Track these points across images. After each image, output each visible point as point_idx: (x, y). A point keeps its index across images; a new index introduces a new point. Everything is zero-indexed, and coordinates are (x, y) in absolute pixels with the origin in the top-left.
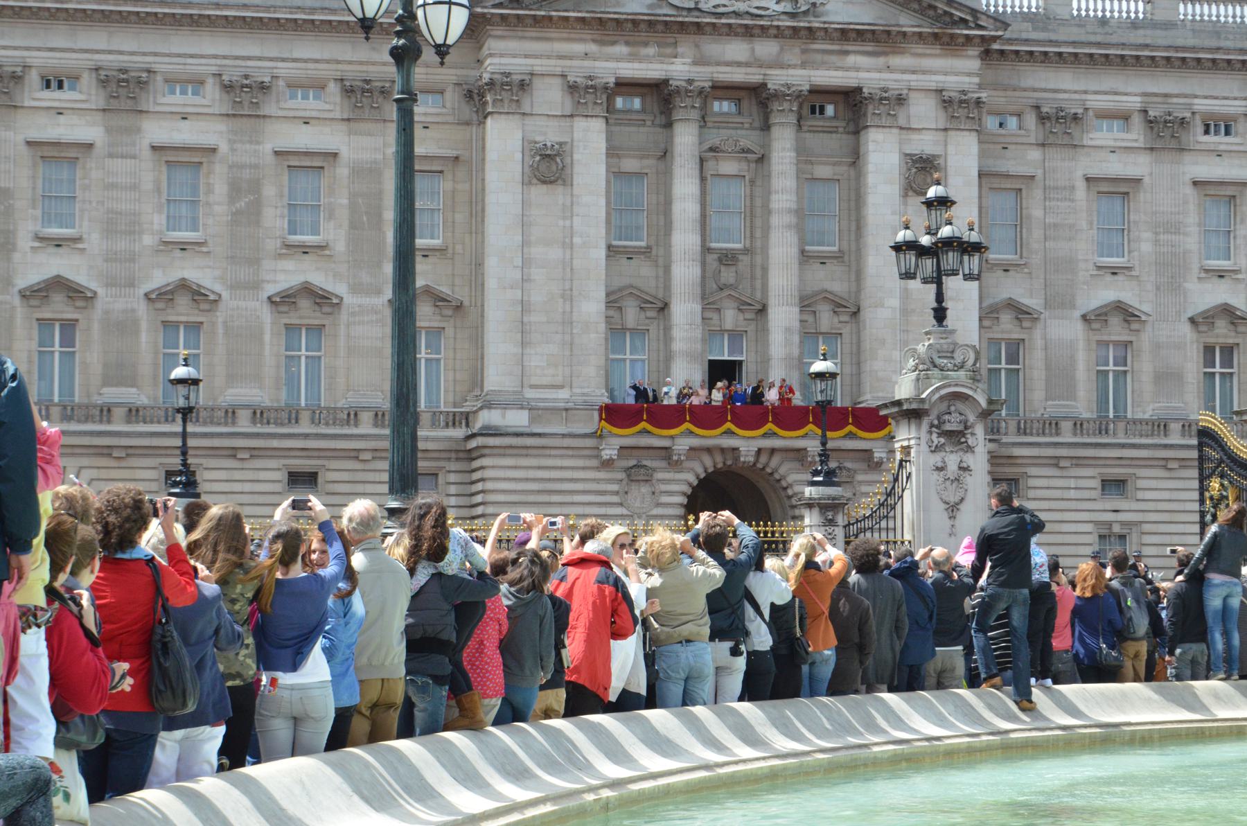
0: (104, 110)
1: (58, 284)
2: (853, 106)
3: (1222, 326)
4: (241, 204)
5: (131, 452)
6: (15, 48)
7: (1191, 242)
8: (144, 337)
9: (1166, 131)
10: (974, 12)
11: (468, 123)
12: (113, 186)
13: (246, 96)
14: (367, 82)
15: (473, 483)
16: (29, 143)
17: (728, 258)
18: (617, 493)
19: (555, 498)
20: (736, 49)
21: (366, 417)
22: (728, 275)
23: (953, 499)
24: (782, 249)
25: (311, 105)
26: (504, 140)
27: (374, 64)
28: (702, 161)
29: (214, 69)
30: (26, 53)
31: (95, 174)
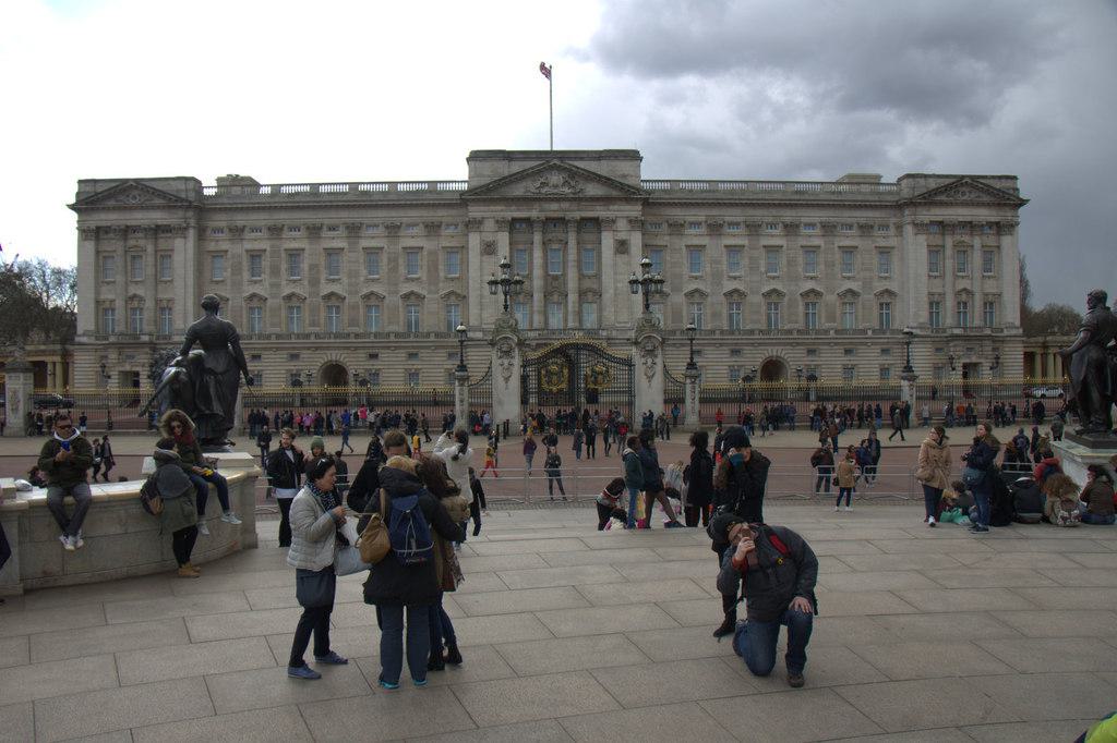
1: (332, 294)
2: (597, 223)
3: (735, 296)
5: (356, 349)
7: (725, 267)
8: (361, 311)
9: (715, 229)
10: (639, 190)
12: (349, 262)
13: (393, 230)
17: (556, 278)
20: (554, 206)
22: (555, 284)
23: (506, 374)
24: (572, 274)
26: (474, 241)
28: (544, 243)
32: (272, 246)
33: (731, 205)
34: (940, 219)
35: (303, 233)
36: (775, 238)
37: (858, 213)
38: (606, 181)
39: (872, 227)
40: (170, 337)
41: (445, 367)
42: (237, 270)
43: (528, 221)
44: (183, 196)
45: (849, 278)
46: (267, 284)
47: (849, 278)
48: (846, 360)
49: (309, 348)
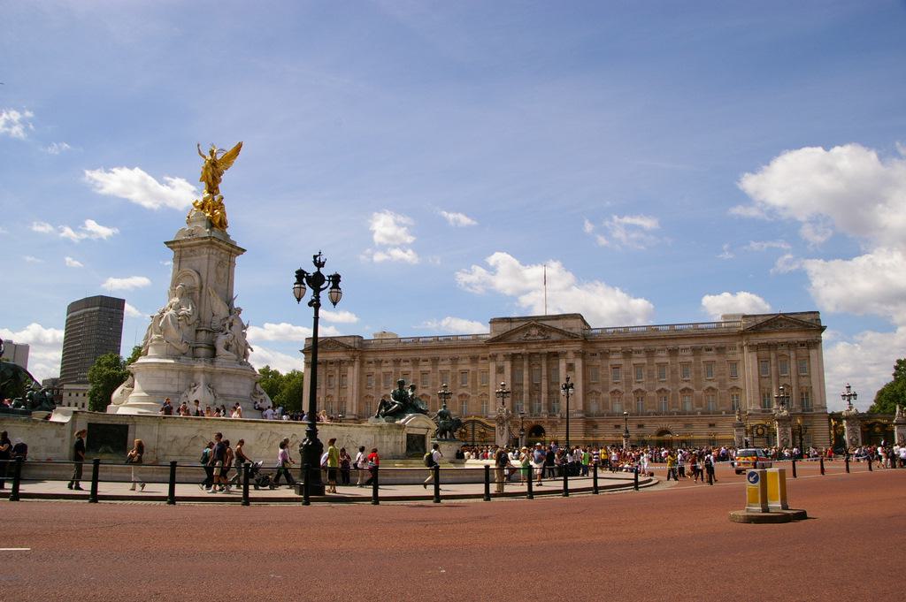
3: (640, 393)
7: (633, 377)
9: (627, 354)
13: (454, 361)
17: (537, 385)
20: (534, 346)
25: (465, 361)
33: (636, 340)
34: (765, 341)
36: (663, 357)
37: (713, 341)
38: (561, 332)
39: (725, 348)
42: (378, 382)
43: (520, 354)
44: (352, 345)
47: (710, 380)
48: (709, 430)
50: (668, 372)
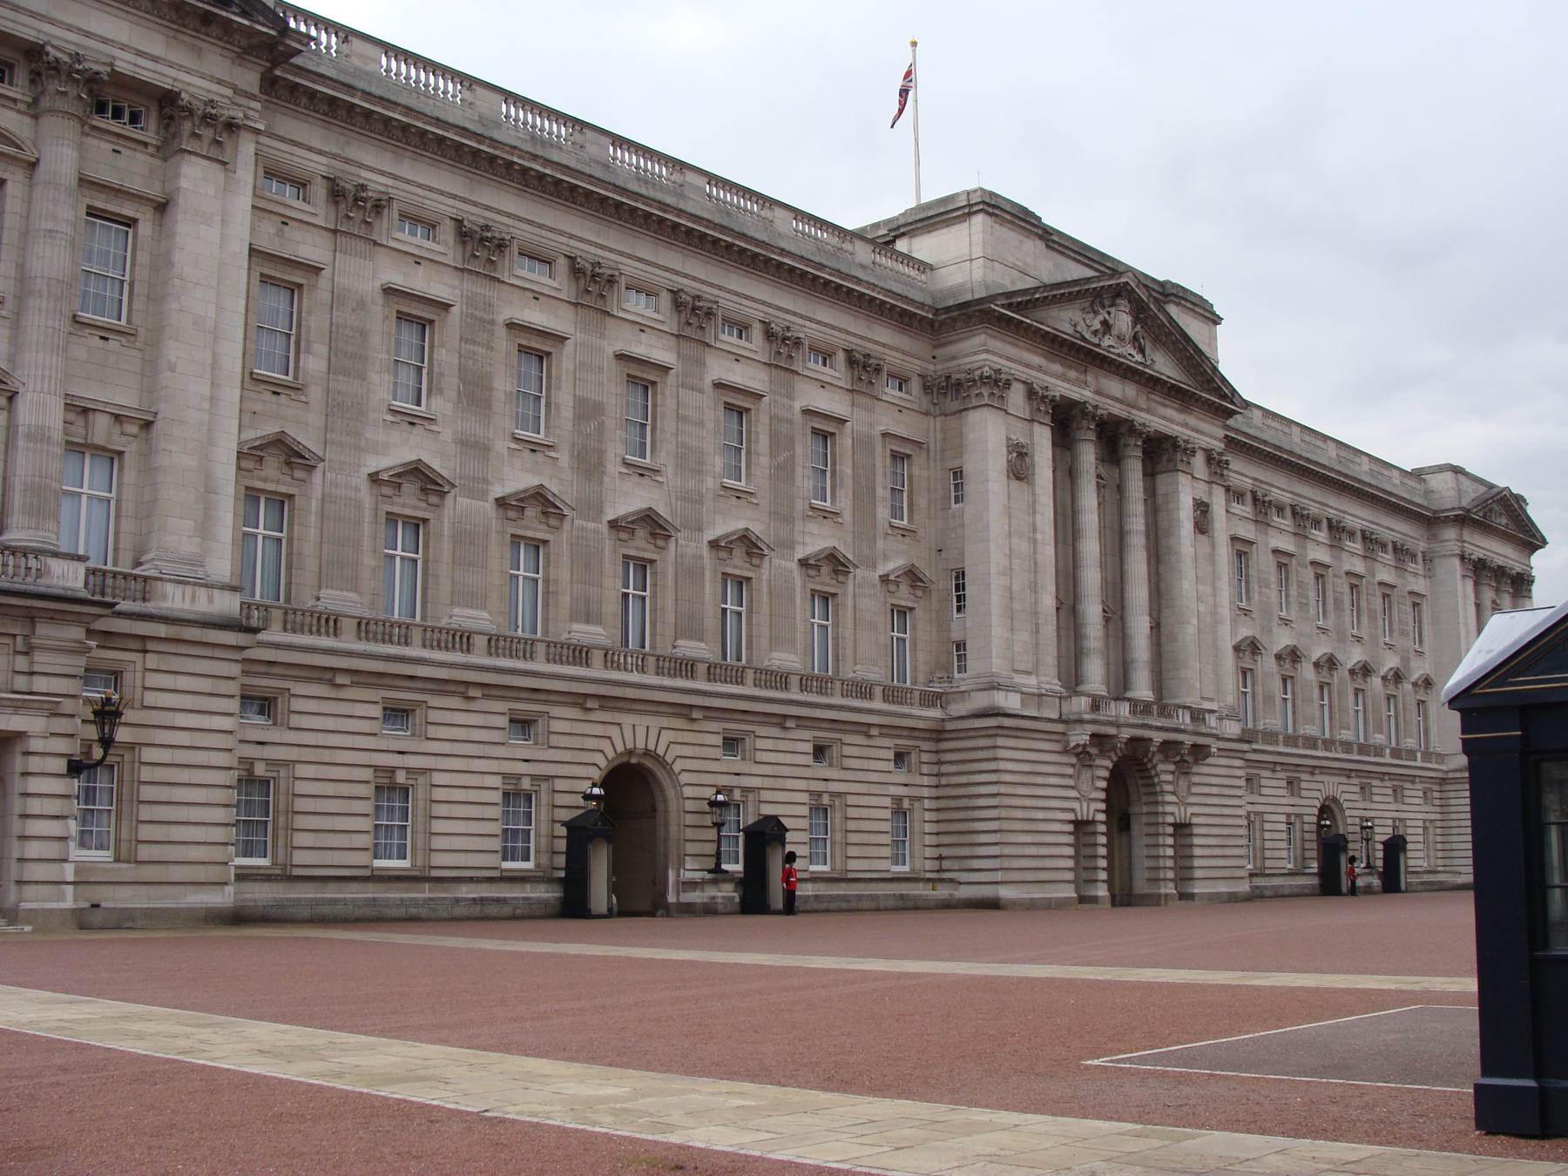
0: (678, 336)
3: (1288, 665)
4: (781, 459)
6: (611, 250)
11: (926, 414)
14: (868, 356)
15: (940, 763)
16: (621, 357)
18: (1070, 776)
19: (1040, 780)
20: (1114, 386)
21: (878, 691)
25: (827, 373)
26: (989, 434)
27: (870, 340)
29: (761, 316)
30: (619, 258)
31: (671, 404)
32: (470, 301)
34: (1478, 554)
35: (559, 283)
40: (145, 586)
41: (894, 790)
42: (347, 359)
45: (1390, 647)
46: (447, 434)
49: (579, 701)
50: (1330, 601)
